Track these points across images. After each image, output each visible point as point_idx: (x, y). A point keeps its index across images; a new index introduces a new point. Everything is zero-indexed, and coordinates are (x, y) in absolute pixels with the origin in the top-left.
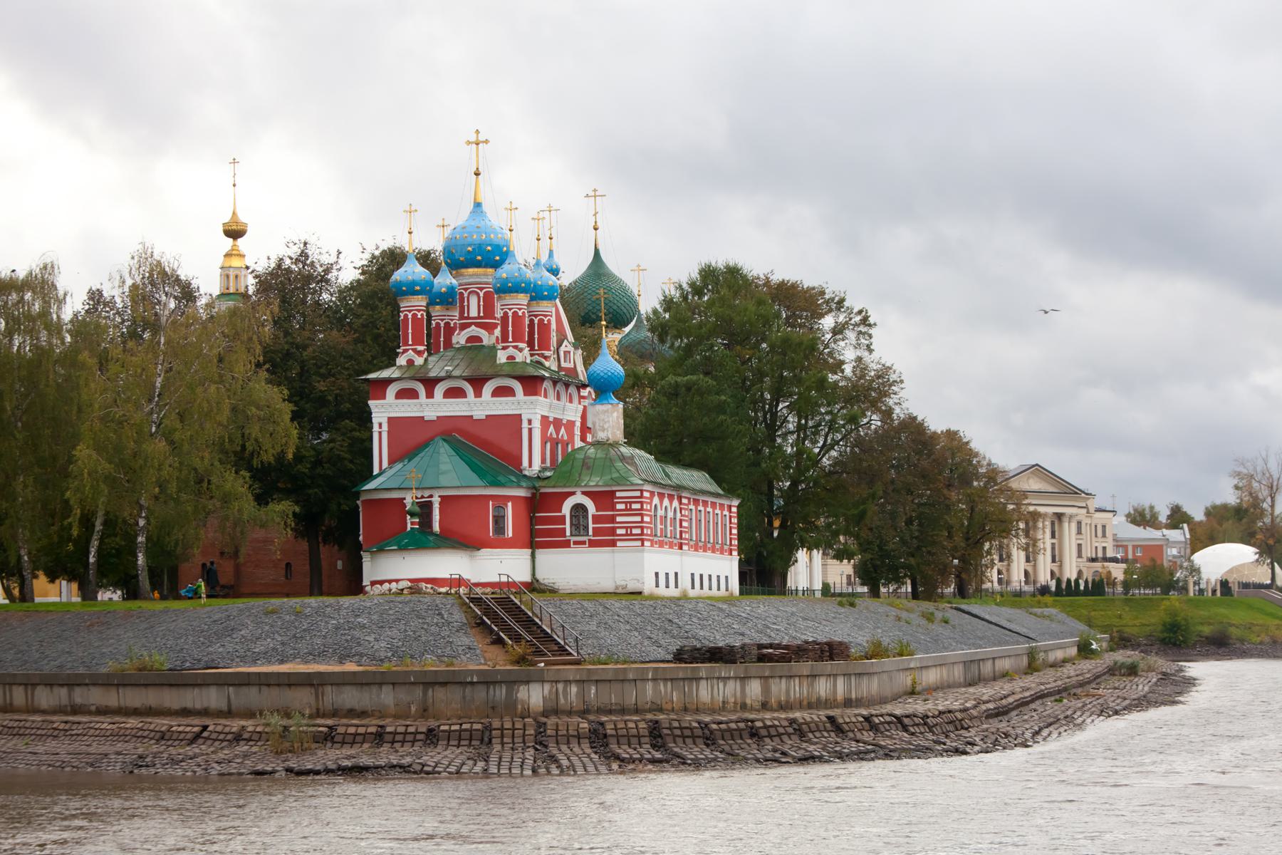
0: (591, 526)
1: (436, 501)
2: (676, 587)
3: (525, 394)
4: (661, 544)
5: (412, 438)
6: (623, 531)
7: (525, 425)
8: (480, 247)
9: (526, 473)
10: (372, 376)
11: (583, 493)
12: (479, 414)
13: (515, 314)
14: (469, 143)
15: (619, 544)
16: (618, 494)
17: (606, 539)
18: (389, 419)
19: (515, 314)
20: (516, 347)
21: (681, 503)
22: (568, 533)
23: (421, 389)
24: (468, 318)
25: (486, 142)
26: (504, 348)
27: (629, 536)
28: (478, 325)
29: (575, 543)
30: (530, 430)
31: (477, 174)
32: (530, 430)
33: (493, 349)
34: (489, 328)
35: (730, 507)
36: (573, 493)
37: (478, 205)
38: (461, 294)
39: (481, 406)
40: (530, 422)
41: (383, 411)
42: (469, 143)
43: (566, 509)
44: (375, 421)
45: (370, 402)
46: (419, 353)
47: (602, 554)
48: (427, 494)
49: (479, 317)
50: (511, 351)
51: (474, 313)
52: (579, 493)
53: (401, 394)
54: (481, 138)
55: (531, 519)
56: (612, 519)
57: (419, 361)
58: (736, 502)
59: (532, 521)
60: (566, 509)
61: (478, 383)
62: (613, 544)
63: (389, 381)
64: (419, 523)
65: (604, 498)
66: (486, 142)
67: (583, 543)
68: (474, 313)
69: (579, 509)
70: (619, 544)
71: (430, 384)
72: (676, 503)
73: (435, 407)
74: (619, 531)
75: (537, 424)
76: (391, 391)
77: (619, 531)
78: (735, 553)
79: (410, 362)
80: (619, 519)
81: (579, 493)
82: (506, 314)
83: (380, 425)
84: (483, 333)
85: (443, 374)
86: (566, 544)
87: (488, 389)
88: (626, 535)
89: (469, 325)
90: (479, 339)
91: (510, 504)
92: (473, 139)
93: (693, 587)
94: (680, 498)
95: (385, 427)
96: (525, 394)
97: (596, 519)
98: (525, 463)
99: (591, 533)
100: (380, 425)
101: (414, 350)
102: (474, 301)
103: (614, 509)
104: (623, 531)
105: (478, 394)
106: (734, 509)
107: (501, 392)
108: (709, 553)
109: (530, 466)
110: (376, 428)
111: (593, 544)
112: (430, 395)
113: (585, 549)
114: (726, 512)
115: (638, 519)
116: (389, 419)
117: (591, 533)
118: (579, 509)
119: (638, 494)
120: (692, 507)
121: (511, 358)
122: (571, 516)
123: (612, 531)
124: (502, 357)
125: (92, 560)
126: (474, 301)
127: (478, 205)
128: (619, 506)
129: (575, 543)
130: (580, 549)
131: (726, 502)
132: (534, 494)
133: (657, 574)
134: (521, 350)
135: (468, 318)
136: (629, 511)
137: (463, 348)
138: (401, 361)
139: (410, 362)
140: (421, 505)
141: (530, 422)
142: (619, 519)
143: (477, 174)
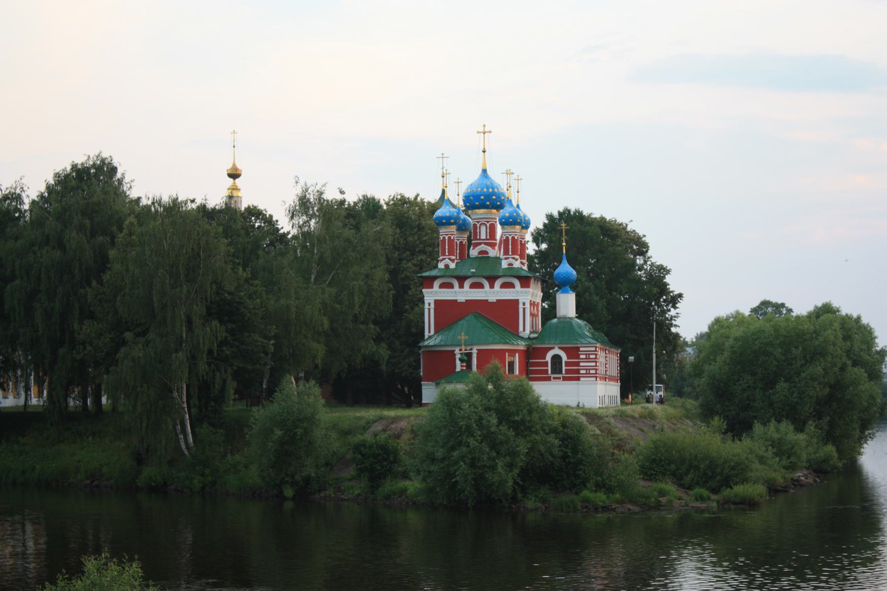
0: (564, 368)
1: (475, 352)
3: (522, 287)
5: (448, 313)
6: (584, 372)
7: (521, 306)
8: (488, 196)
9: (521, 335)
10: (424, 274)
11: (560, 348)
12: (492, 298)
13: (513, 238)
14: (478, 132)
16: (581, 349)
17: (574, 376)
18: (436, 302)
19: (513, 238)
20: (513, 258)
22: (550, 372)
23: (456, 283)
24: (480, 239)
25: (490, 132)
26: (506, 259)
27: (588, 374)
28: (485, 244)
29: (554, 378)
30: (524, 309)
31: (484, 152)
32: (524, 309)
33: (498, 260)
34: (493, 245)
36: (553, 348)
37: (484, 171)
38: (475, 225)
39: (493, 294)
40: (524, 304)
41: (432, 295)
42: (478, 132)
43: (548, 358)
44: (426, 302)
45: (424, 290)
46: (453, 261)
47: (571, 386)
48: (468, 348)
49: (487, 239)
50: (511, 261)
51: (483, 236)
53: (442, 286)
54: (487, 129)
55: (527, 363)
56: (578, 364)
57: (452, 266)
59: (528, 364)
60: (548, 358)
61: (492, 280)
62: (578, 379)
63: (435, 278)
64: (466, 366)
65: (573, 352)
66: (490, 132)
67: (559, 378)
68: (483, 236)
69: (556, 359)
70: (582, 379)
71: (461, 280)
73: (463, 294)
75: (528, 305)
76: (437, 284)
77: (582, 372)
79: (447, 266)
80: (581, 364)
82: (507, 238)
83: (429, 304)
84: (489, 249)
85: (469, 274)
86: (549, 379)
87: (498, 283)
89: (480, 244)
90: (486, 253)
92: (482, 130)
95: (432, 306)
96: (522, 287)
97: (567, 364)
98: (521, 328)
100: (429, 304)
101: (450, 259)
102: (483, 229)
103: (579, 358)
104: (584, 372)
105: (492, 286)
107: (504, 286)
109: (524, 330)
110: (426, 306)
111: (565, 379)
112: (461, 286)
113: (560, 382)
115: (594, 364)
116: (436, 302)
118: (556, 359)
119: (594, 349)
121: (510, 264)
123: (578, 371)
124: (504, 264)
125: (264, 386)
126: (483, 229)
127: (484, 171)
128: (582, 357)
129: (554, 378)
130: (557, 381)
132: (528, 348)
134: (516, 260)
135: (480, 239)
136: (588, 359)
137: (476, 258)
138: (441, 265)
139: (447, 266)
140: (466, 354)
141: (524, 304)
142: (581, 364)
143: (484, 152)
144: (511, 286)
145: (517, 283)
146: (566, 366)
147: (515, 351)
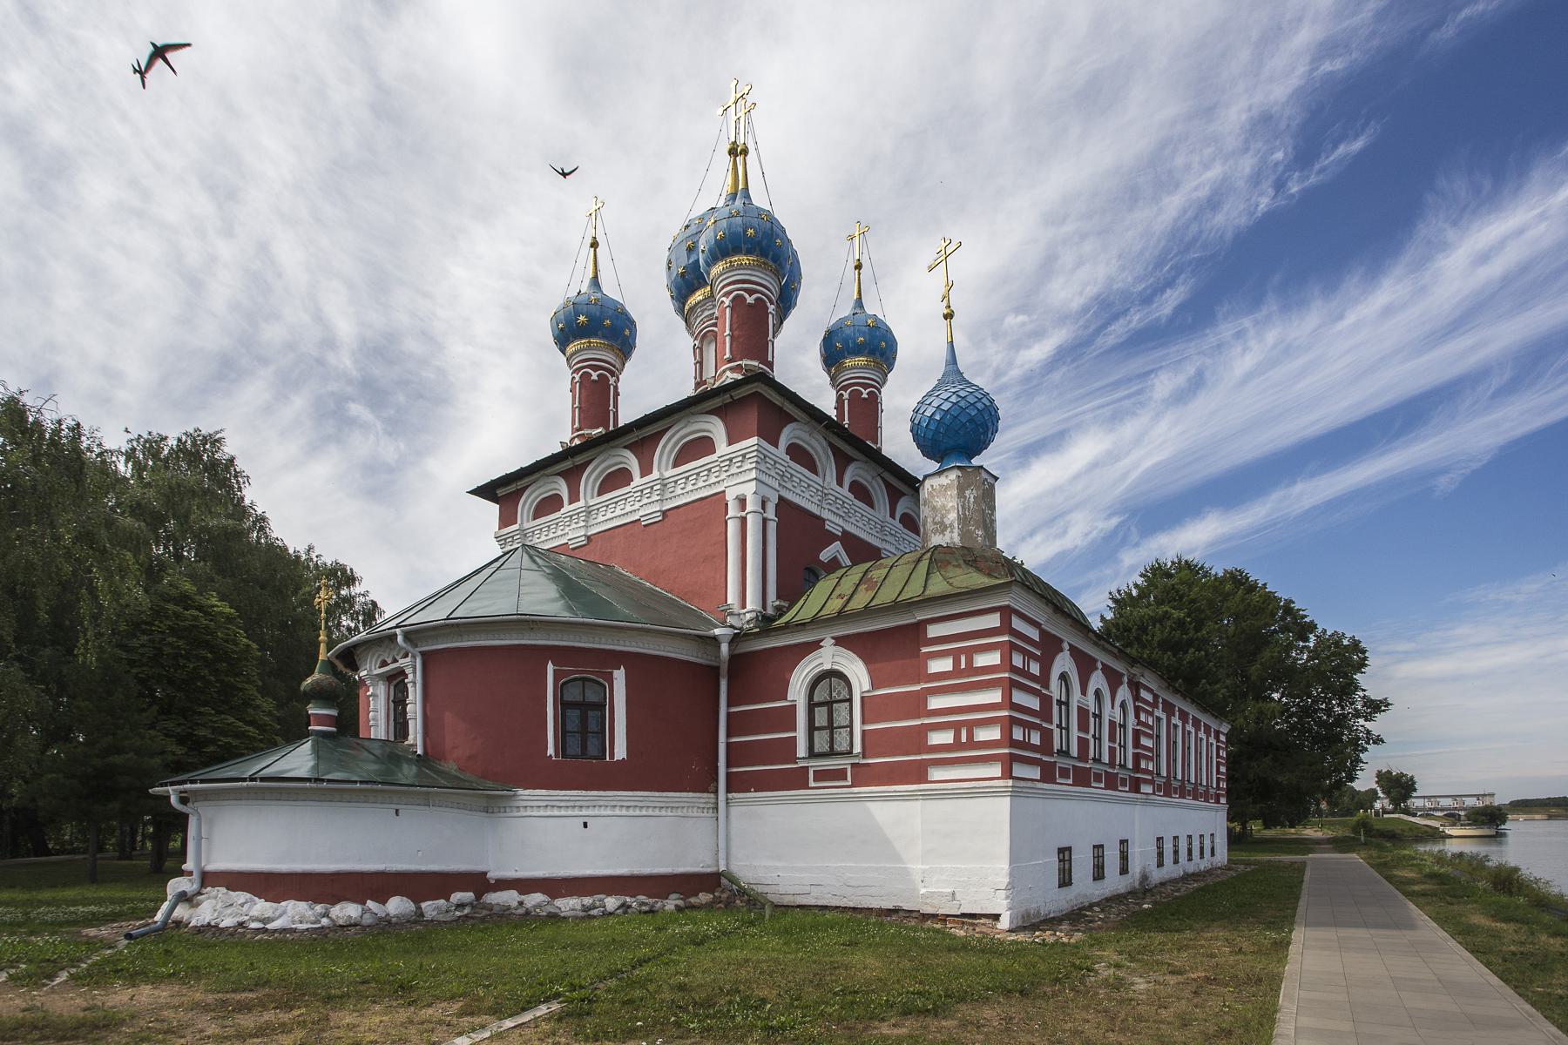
2: (1124, 870)
4: (1082, 778)
6: (946, 737)
7: (733, 511)
11: (840, 641)
15: (936, 774)
17: (900, 763)
21: (1137, 698)
27: (965, 751)
35: (1217, 733)
36: (816, 645)
40: (742, 502)
52: (828, 643)
56: (916, 705)
58: (1225, 728)
62: (917, 774)
72: (1124, 693)
74: (936, 738)
77: (936, 738)
78: (1223, 800)
81: (828, 643)
88: (957, 745)
91: (619, 676)
93: (1160, 864)
94: (1135, 687)
98: (732, 598)
99: (857, 749)
103: (922, 675)
104: (946, 737)
106: (1223, 738)
108: (1189, 801)
114: (1212, 740)
117: (857, 749)
120: (1159, 713)
122: (812, 707)
123: (916, 740)
131: (1214, 725)
133: (1065, 853)
142: (935, 703)
144: (703, 446)
145: (716, 429)
146: (863, 722)
147: (617, 658)
